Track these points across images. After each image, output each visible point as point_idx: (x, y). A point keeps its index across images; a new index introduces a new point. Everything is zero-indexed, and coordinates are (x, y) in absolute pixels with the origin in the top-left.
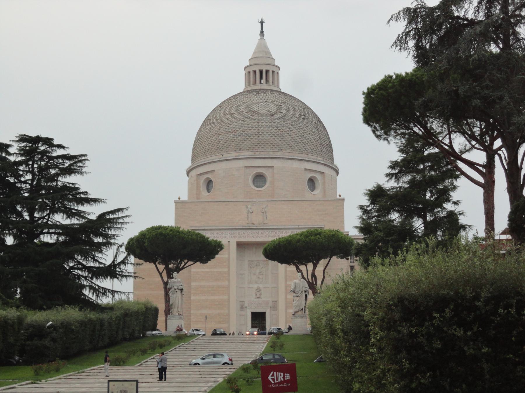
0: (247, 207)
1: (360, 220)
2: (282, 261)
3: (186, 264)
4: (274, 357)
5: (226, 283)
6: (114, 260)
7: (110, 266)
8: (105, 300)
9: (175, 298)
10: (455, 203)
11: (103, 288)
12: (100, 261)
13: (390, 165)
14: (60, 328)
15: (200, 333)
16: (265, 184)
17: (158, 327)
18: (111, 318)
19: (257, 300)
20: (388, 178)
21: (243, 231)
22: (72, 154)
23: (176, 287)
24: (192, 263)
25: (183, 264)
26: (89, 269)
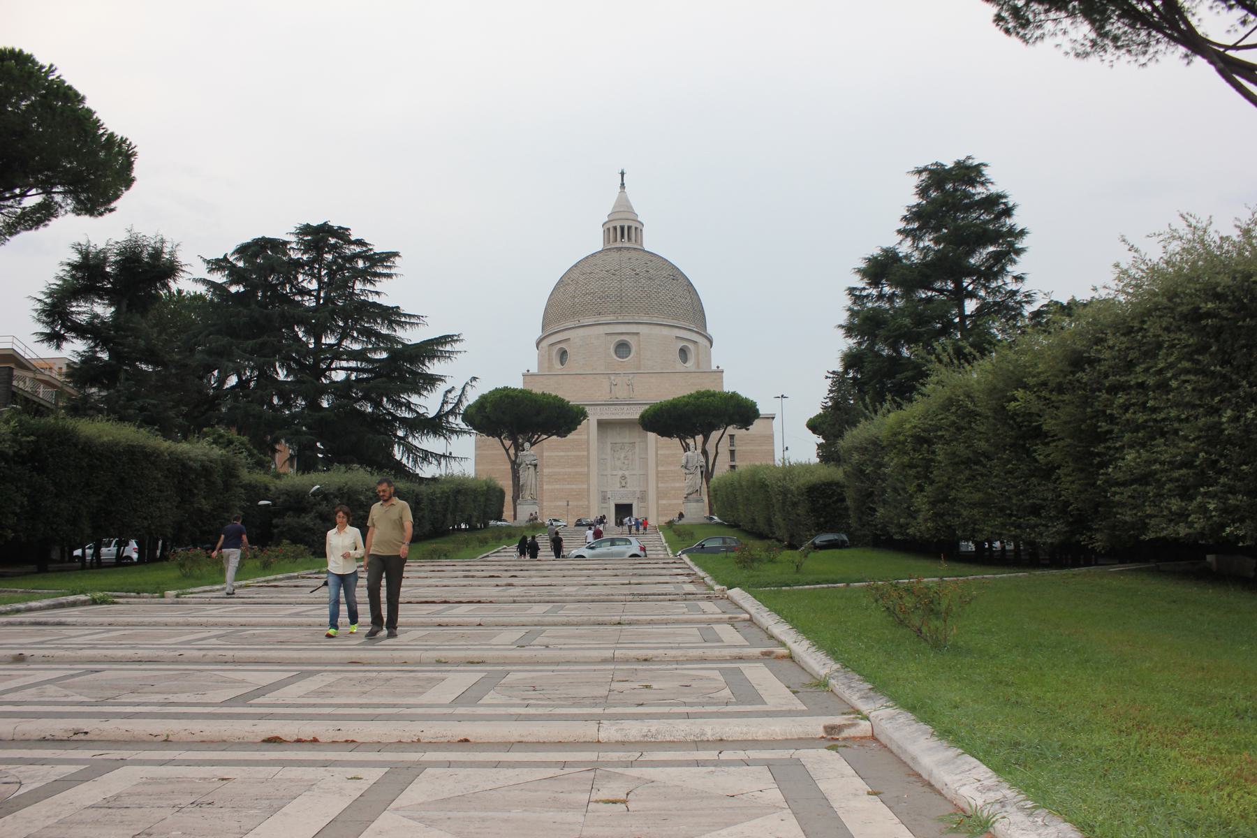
0: (610, 378)
1: (848, 313)
2: (664, 431)
3: (539, 436)
4: (724, 542)
5: (586, 469)
6: (440, 411)
7: (433, 418)
8: (427, 471)
9: (527, 476)
10: (1019, 279)
11: (423, 450)
12: (418, 410)
13: (906, 213)
14: (336, 497)
15: (559, 524)
16: (630, 351)
17: (504, 517)
18: (433, 493)
19: (622, 489)
20: (900, 237)
21: (605, 407)
22: (378, 249)
23: (528, 463)
24: (545, 437)
25: (536, 436)
26: (404, 421)
